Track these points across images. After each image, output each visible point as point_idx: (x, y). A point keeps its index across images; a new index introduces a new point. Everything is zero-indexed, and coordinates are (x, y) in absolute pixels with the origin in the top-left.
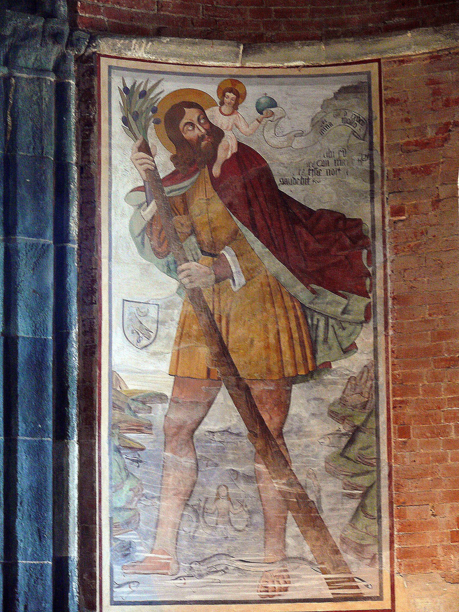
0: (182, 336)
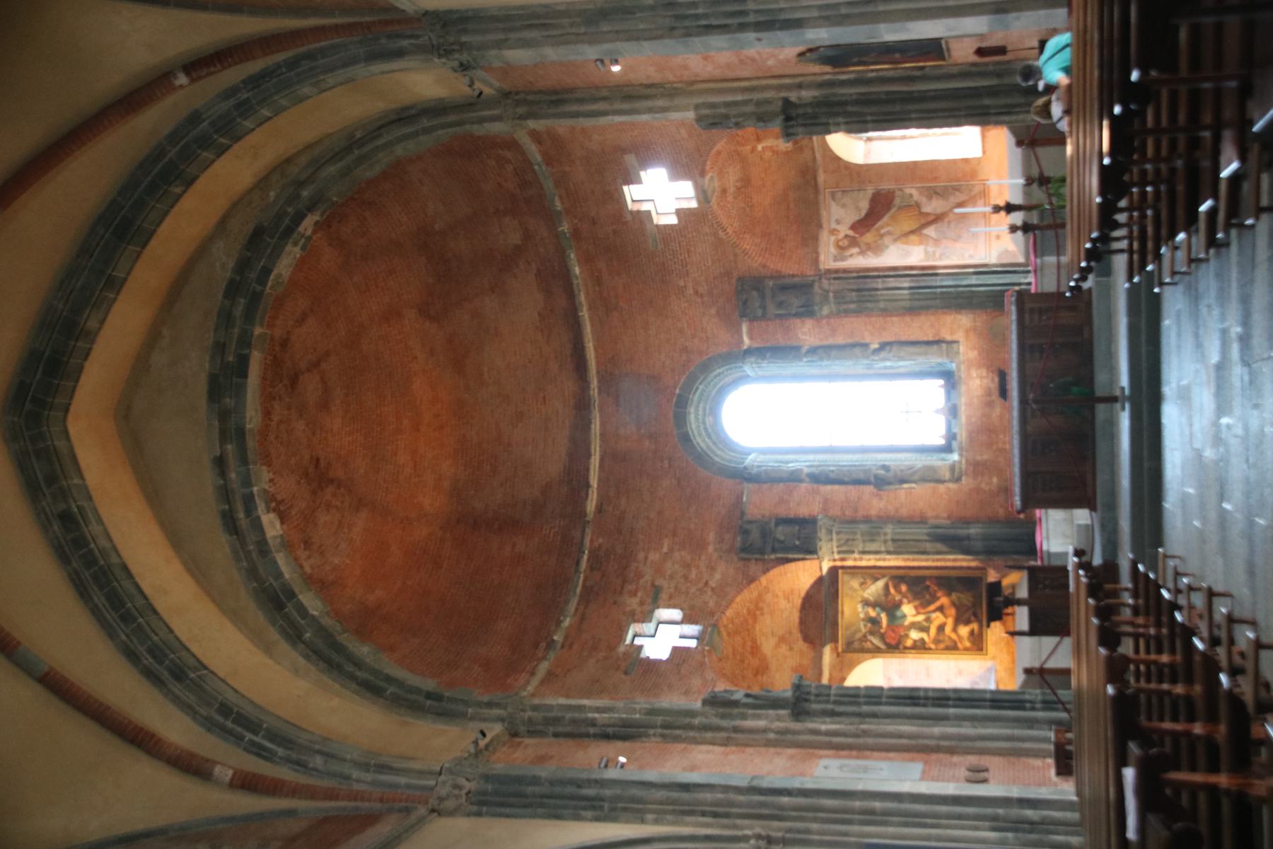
0: (906, 243)
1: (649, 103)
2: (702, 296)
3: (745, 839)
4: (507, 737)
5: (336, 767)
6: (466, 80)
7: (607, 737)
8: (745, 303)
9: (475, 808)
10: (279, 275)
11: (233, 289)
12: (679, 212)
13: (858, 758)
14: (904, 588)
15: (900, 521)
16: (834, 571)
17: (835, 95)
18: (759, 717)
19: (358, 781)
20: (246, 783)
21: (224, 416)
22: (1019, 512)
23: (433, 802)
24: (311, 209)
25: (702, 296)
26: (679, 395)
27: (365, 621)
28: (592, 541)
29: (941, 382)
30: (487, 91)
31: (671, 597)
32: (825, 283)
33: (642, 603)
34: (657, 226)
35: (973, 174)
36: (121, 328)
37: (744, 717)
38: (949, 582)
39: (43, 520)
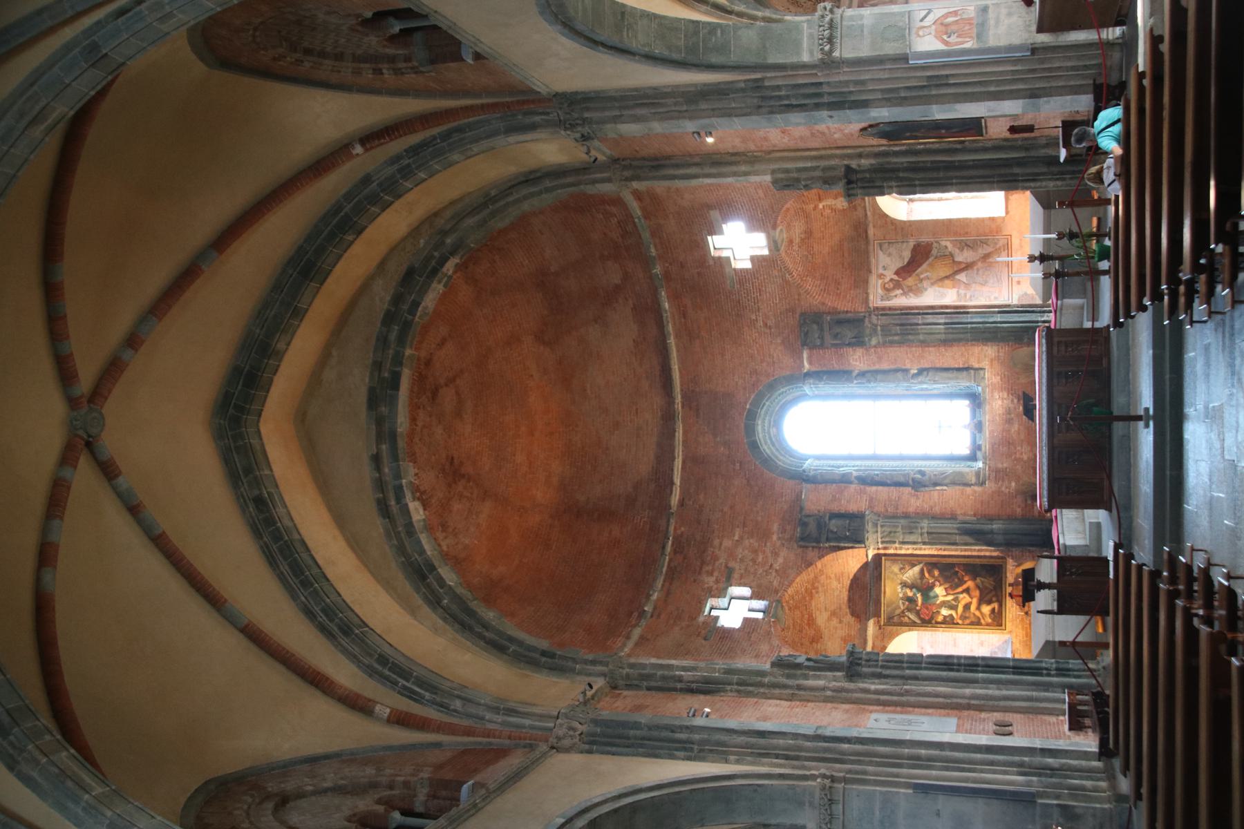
1: (734, 168)
2: (770, 328)
3: (813, 777)
4: (607, 690)
5: (472, 710)
6: (585, 149)
7: (691, 691)
8: (806, 334)
9: (587, 747)
10: (426, 308)
11: (389, 319)
12: (753, 259)
13: (901, 713)
14: (936, 573)
15: (935, 518)
16: (878, 558)
17: (889, 163)
18: (819, 677)
19: (489, 721)
20: (401, 720)
21: (379, 421)
22: (1046, 511)
23: (552, 740)
24: (453, 253)
25: (770, 328)
26: (749, 410)
27: (491, 592)
28: (675, 529)
29: (967, 402)
30: (601, 158)
31: (741, 577)
32: (874, 318)
33: (717, 581)
34: (735, 270)
35: (999, 230)
36: (302, 347)
37: (806, 677)
38: (977, 569)
39: (242, 502)
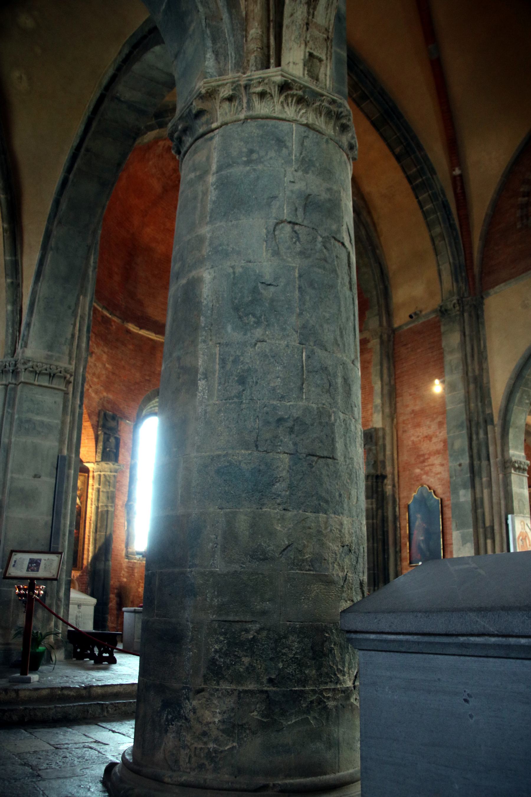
16: (86, 470)
28: (114, 322)
